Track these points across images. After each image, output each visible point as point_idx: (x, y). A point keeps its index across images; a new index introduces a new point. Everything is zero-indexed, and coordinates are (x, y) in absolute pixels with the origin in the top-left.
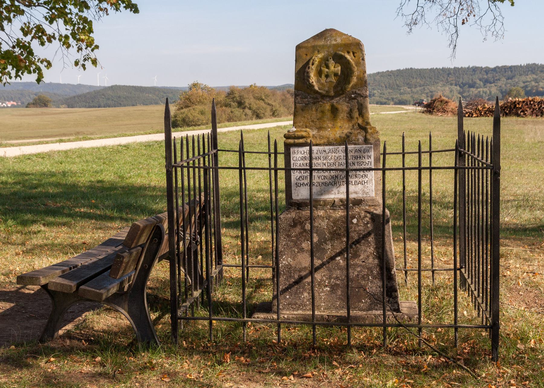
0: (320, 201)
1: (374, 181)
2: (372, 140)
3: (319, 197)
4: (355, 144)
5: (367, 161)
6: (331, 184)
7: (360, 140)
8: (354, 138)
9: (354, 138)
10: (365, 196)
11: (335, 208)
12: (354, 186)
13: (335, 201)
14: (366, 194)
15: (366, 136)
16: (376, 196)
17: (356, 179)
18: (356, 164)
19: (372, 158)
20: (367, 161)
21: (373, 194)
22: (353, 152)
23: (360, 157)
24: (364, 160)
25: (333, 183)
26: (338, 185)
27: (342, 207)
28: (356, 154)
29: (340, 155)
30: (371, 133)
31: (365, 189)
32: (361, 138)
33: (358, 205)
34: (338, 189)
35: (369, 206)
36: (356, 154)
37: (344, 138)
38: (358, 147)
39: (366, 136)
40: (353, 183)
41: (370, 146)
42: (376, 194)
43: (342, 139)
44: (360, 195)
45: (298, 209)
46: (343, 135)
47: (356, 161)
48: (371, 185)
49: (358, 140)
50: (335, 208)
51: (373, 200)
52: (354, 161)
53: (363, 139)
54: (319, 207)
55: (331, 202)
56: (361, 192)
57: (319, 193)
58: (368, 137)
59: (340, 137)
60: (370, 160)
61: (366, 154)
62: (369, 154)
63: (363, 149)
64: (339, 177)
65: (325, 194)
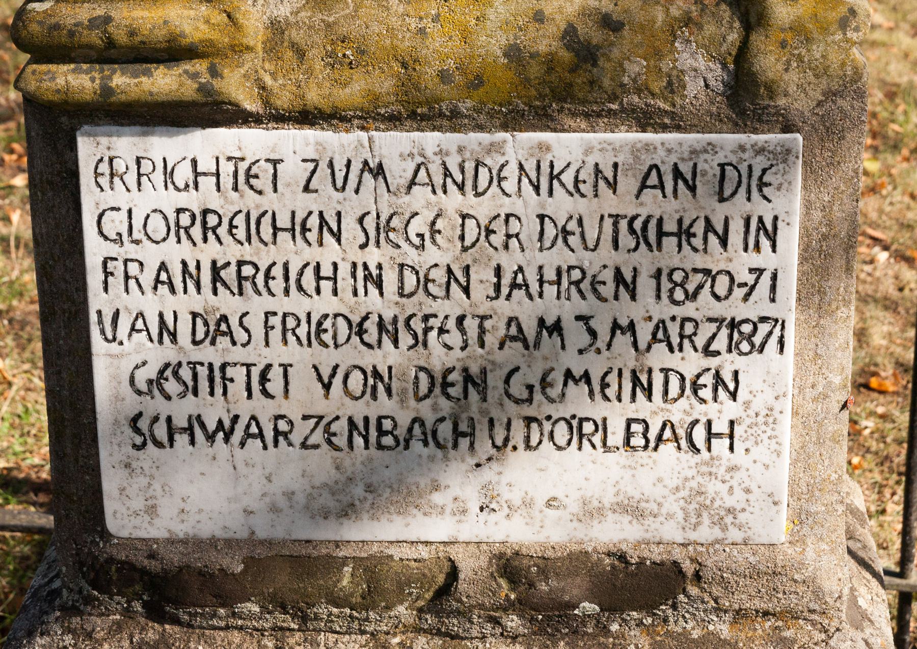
0: (332, 564)
1: (786, 421)
2: (797, 93)
3: (325, 532)
4: (645, 120)
5: (741, 263)
6: (431, 437)
7: (694, 87)
8: (636, 67)
9: (636, 67)
10: (706, 533)
11: (454, 626)
12: (622, 456)
13: (453, 573)
14: (719, 522)
15: (743, 53)
16: (796, 540)
17: (642, 408)
18: (645, 285)
19: (791, 239)
20: (741, 263)
21: (774, 527)
22: (628, 184)
23: (684, 233)
24: (715, 259)
25: (445, 430)
26: (485, 448)
27: (513, 622)
28: (652, 204)
29: (507, 205)
30: (797, 28)
31: (713, 487)
32: (699, 69)
33: (649, 607)
34: (488, 474)
35: (740, 615)
36: (652, 204)
37: (550, 62)
38: (667, 144)
39: (743, 53)
40: (616, 437)
41: (772, 138)
42: (800, 518)
43: (535, 70)
44: (672, 532)
45: (156, 613)
46: (545, 42)
47: (645, 261)
48: (761, 452)
49: (674, 85)
50: (454, 626)
51: (771, 574)
52: (626, 262)
53: (716, 74)
54: (323, 610)
55: (423, 580)
56: (673, 505)
57: (327, 500)
58: (768, 61)
59: (513, 53)
60: (765, 259)
61: (737, 208)
62: (761, 209)
63: (709, 166)
64: (495, 380)
65: (375, 511)
